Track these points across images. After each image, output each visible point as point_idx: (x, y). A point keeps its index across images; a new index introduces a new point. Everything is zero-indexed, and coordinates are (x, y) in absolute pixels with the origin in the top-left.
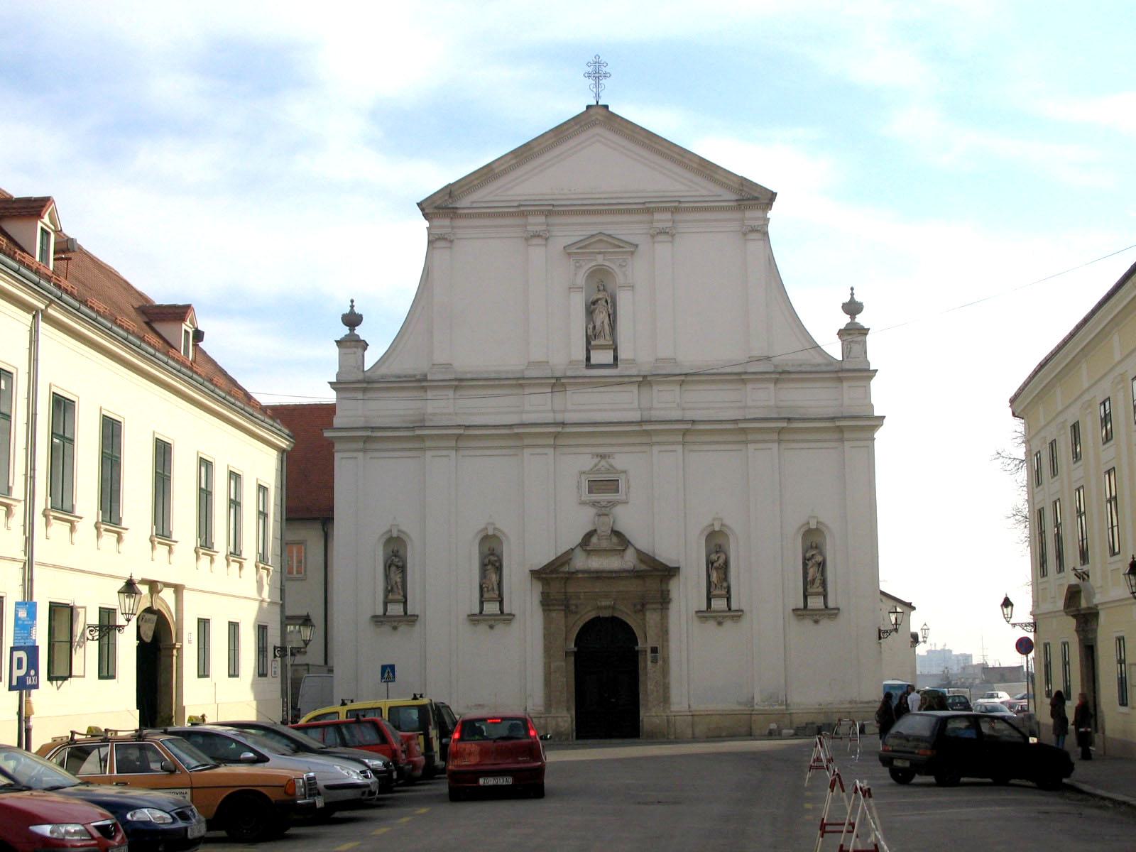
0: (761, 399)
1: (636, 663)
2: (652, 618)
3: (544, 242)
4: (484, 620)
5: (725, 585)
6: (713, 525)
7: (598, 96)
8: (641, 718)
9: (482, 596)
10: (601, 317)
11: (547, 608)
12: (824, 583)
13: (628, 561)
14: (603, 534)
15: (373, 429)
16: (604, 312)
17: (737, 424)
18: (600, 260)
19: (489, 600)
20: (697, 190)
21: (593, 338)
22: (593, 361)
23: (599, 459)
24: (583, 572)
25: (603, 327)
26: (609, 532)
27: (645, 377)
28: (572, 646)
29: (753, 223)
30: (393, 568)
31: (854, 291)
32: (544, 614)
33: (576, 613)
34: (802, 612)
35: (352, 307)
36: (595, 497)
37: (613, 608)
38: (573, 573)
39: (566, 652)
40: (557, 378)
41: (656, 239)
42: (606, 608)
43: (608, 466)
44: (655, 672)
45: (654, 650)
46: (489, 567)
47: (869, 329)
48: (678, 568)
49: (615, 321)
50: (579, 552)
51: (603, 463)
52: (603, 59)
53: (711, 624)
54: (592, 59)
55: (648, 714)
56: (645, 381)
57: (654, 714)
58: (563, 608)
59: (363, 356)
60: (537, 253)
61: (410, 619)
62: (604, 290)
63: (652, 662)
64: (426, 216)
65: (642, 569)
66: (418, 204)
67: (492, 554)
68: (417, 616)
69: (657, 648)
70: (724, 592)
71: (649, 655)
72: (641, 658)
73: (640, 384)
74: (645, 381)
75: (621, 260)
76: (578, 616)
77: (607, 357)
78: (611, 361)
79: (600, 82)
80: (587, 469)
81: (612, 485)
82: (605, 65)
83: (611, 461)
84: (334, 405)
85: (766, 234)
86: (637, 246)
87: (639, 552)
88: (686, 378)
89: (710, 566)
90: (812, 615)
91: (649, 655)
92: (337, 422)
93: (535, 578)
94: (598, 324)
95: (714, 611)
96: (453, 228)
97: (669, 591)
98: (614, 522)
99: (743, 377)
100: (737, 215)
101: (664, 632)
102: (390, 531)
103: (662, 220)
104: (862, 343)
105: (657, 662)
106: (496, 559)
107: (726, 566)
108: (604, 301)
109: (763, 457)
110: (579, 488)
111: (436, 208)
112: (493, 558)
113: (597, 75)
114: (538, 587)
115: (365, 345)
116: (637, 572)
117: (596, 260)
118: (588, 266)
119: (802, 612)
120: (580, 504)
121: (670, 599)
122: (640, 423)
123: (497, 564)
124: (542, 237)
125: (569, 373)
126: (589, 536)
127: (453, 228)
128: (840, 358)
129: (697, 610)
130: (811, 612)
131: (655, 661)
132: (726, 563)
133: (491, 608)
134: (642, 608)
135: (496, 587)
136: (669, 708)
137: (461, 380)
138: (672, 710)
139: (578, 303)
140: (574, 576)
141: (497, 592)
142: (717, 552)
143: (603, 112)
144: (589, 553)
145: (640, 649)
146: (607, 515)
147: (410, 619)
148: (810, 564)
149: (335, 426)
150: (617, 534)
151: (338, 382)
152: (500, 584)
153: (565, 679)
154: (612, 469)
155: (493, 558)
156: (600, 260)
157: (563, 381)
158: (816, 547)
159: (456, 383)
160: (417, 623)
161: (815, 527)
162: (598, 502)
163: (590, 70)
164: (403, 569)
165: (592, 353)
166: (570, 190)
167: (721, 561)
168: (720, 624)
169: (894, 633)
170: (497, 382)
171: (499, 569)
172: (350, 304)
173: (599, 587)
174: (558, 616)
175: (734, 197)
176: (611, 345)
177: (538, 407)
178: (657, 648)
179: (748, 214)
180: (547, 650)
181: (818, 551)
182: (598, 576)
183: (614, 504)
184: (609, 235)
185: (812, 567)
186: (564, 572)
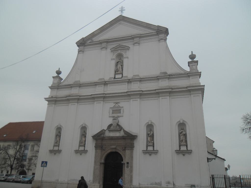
0: (164, 84)
2: (128, 152)
4: (79, 152)
5: (152, 142)
10: (119, 66)
12: (186, 141)
13: (122, 134)
14: (114, 125)
18: (119, 52)
26: (116, 125)
27: (129, 80)
28: (103, 161)
30: (58, 136)
32: (95, 150)
33: (104, 150)
34: (179, 152)
35: (59, 69)
36: (114, 115)
37: (115, 148)
39: (100, 163)
44: (127, 171)
45: (128, 163)
46: (83, 136)
48: (137, 136)
51: (117, 105)
52: (124, 6)
53: (147, 155)
54: (121, 7)
56: (129, 81)
58: (100, 148)
60: (104, 52)
63: (127, 167)
64: (78, 46)
65: (125, 136)
68: (61, 150)
69: (128, 162)
70: (152, 144)
71: (126, 165)
72: (124, 166)
74: (129, 81)
77: (120, 76)
78: (121, 77)
80: (112, 106)
83: (119, 104)
88: (141, 80)
90: (182, 152)
91: (126, 165)
94: (118, 68)
95: (148, 151)
96: (84, 48)
97: (134, 143)
99: (158, 77)
100: (157, 37)
101: (132, 157)
102: (58, 126)
103: (136, 40)
105: (128, 167)
108: (120, 62)
109: (165, 101)
111: (81, 43)
117: (118, 52)
119: (179, 152)
120: (109, 117)
121: (134, 146)
122: (127, 92)
126: (110, 126)
127: (84, 48)
132: (153, 135)
133: (82, 148)
136: (132, 185)
139: (113, 63)
141: (84, 143)
142: (150, 131)
144: (110, 131)
148: (181, 135)
152: (85, 141)
154: (120, 107)
155: (84, 133)
156: (119, 52)
157: (107, 82)
158: (183, 129)
161: (182, 122)
163: (120, 9)
164: (60, 136)
168: (150, 155)
169: (213, 160)
171: (85, 137)
174: (99, 151)
175: (156, 32)
177: (99, 90)
178: (128, 162)
179: (160, 36)
180: (95, 162)
181: (183, 130)
182: (112, 138)
183: (119, 117)
185: (181, 136)
186: (101, 137)
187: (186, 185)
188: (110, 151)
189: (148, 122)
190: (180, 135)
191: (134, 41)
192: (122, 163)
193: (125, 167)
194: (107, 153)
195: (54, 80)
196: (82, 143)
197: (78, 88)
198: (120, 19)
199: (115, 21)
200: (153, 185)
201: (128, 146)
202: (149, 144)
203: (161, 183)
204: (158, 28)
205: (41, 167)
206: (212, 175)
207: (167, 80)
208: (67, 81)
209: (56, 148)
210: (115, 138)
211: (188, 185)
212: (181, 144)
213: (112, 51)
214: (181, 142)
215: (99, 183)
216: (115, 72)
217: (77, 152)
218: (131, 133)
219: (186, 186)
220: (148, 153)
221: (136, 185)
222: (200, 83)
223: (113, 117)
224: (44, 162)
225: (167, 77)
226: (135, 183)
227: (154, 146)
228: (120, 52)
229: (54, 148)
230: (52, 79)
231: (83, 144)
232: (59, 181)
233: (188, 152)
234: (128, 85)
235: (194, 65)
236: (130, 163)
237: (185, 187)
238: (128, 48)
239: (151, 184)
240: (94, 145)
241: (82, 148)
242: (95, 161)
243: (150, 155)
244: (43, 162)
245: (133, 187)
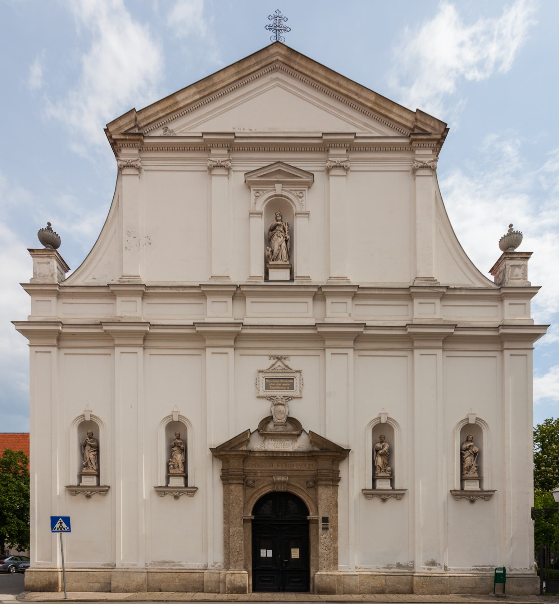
52: (283, 14)
54: (273, 13)
80: (265, 367)
113: (278, 28)
146: (283, 405)
150: (291, 421)
163: (272, 22)
188: (270, 490)
198: (274, 59)
199: (257, 67)
234: (313, 309)
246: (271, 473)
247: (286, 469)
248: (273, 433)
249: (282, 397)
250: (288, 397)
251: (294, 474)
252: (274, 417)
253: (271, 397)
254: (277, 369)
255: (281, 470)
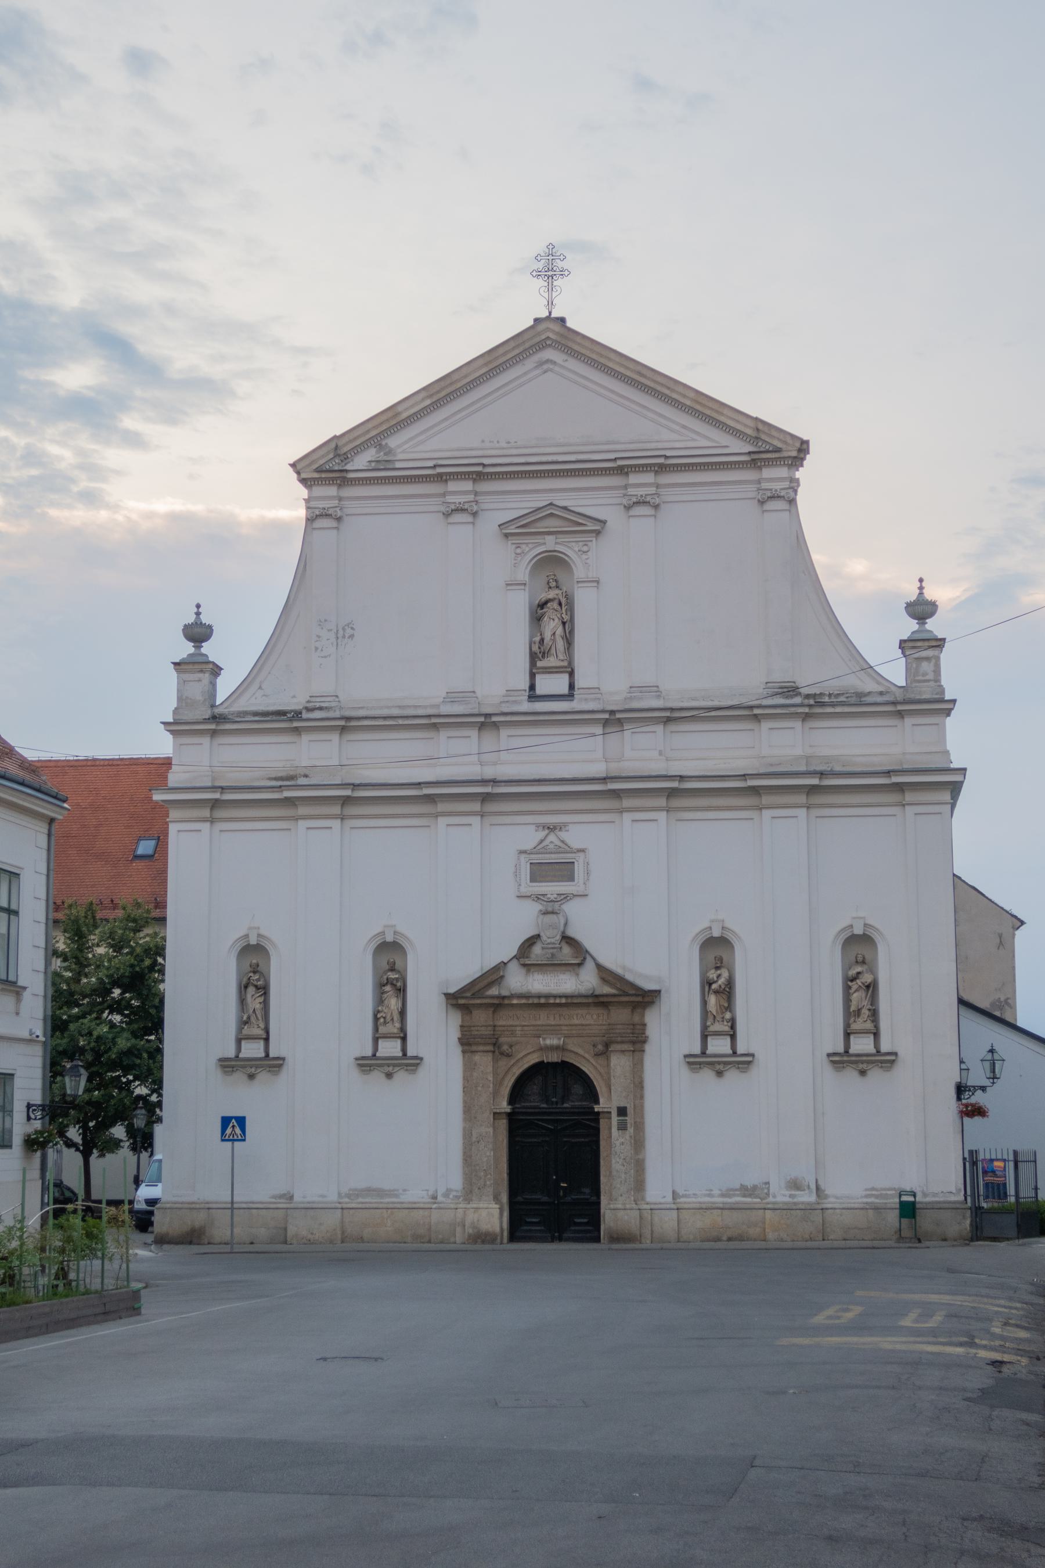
1: (594, 1133)
2: (620, 1063)
3: (470, 519)
5: (728, 1015)
6: (710, 928)
7: (550, 303)
8: (602, 1211)
9: (376, 1029)
10: (551, 626)
11: (466, 1048)
12: (874, 1014)
13: (586, 981)
14: (549, 941)
15: (222, 789)
16: (557, 620)
17: (746, 780)
18: (550, 543)
19: (386, 1037)
20: (693, 440)
21: (540, 656)
22: (539, 691)
23: (547, 831)
24: (520, 996)
25: (554, 641)
26: (559, 937)
28: (504, 1106)
29: (777, 486)
30: (251, 990)
31: (924, 584)
32: (464, 1057)
33: (508, 1056)
35: (198, 614)
37: (561, 1048)
38: (504, 997)
39: (495, 1114)
40: (488, 716)
41: (632, 512)
42: (556, 1048)
43: (559, 843)
44: (623, 1144)
46: (388, 988)
47: (944, 640)
49: (572, 631)
50: (514, 969)
51: (552, 838)
53: (708, 1074)
54: (541, 248)
55: (612, 1206)
57: (620, 1206)
59: (213, 685)
60: (460, 532)
61: (273, 1064)
62: (557, 587)
64: (303, 481)
66: (291, 465)
67: (392, 969)
68: (283, 1059)
69: (625, 1108)
70: (726, 1028)
72: (603, 1123)
73: (606, 723)
75: (581, 543)
76: (512, 1063)
78: (565, 690)
79: (555, 283)
80: (529, 846)
81: (564, 871)
82: (562, 257)
83: (563, 835)
84: (169, 759)
85: (792, 502)
86: (604, 522)
87: (600, 967)
89: (707, 988)
90: (856, 1062)
91: (615, 1119)
92: (175, 778)
93: (453, 1005)
94: (548, 636)
97: (645, 1025)
98: (566, 924)
99: (756, 711)
100: (750, 475)
101: (638, 1085)
102: (247, 936)
103: (641, 483)
104: (933, 661)
106: (397, 976)
107: (730, 988)
108: (556, 602)
110: (516, 874)
111: (318, 470)
112: (393, 976)
113: (550, 273)
114: (455, 1019)
115: (216, 670)
116: (594, 996)
117: (545, 544)
118: (533, 550)
120: (518, 897)
122: (604, 780)
123: (399, 984)
124: (471, 512)
125: (505, 709)
126: (531, 941)
128: (901, 682)
129: (687, 1053)
130: (853, 1058)
131: (622, 1127)
132: (730, 984)
133: (390, 1048)
134: (604, 1052)
135: (396, 1017)
136: (643, 1199)
137: (348, 719)
138: (648, 1199)
139: (520, 603)
140: (506, 1002)
141: (398, 1025)
142: (717, 968)
143: (556, 327)
144: (528, 967)
145: (600, 1110)
147: (273, 1064)
148: (854, 986)
149: (171, 784)
151: (175, 723)
152: (403, 1013)
153: (492, 1154)
154: (565, 848)
155: (393, 976)
156: (550, 543)
158: (864, 962)
159: (342, 723)
160: (285, 1068)
161: (861, 932)
162: (543, 895)
163: (540, 265)
164: (264, 990)
165: (538, 677)
166: (509, 443)
167: (721, 981)
168: (720, 1074)
170: (401, 722)
171: (401, 991)
172: (195, 610)
173: (544, 1018)
174: (484, 1061)
176: (566, 667)
178: (625, 1108)
180: (469, 1111)
183: (566, 897)
184: (565, 508)
185: (855, 992)
186: (492, 997)
187: (866, 1190)
188: (537, 1060)
189: (710, 928)
190: (850, 987)
191: (631, 491)
192: (596, 1110)
193: (610, 1128)
194: (521, 1070)
195: (182, 684)
196: (385, 1023)
197: (335, 737)
198: (543, 337)
200: (734, 1195)
201: (619, 1039)
202: (712, 1029)
203: (768, 1189)
204: (758, 430)
205: (223, 1140)
206: (971, 1152)
207: (798, 724)
208: (260, 688)
209: (253, 1050)
210: (558, 1001)
211: (876, 1190)
212: (855, 1027)
213: (506, 535)
214: (852, 1020)
215: (496, 1198)
216: (533, 657)
217: (367, 1064)
218: (629, 977)
219: (867, 1196)
220: (711, 1064)
221: (663, 1200)
222: (947, 753)
223: (538, 898)
224: (233, 1121)
225: (800, 710)
226: (656, 1191)
227: (733, 1037)
228: (556, 543)
229: (239, 1049)
230: (173, 675)
231: (394, 1028)
232: (296, 1198)
233: (882, 1062)
235: (928, 659)
236: (630, 1111)
237: (862, 1197)
238: (597, 528)
239: (723, 1195)
240: (455, 1034)
241: (390, 1048)
242: (465, 1107)
243: (720, 1074)
244: (226, 1121)
245: (648, 1207)
246: (537, 1030)
247: (561, 1022)
248: (540, 962)
249: (555, 896)
250: (565, 896)
251: (574, 1032)
252: (542, 934)
253: (539, 897)
254: (548, 847)
255: (554, 1025)
